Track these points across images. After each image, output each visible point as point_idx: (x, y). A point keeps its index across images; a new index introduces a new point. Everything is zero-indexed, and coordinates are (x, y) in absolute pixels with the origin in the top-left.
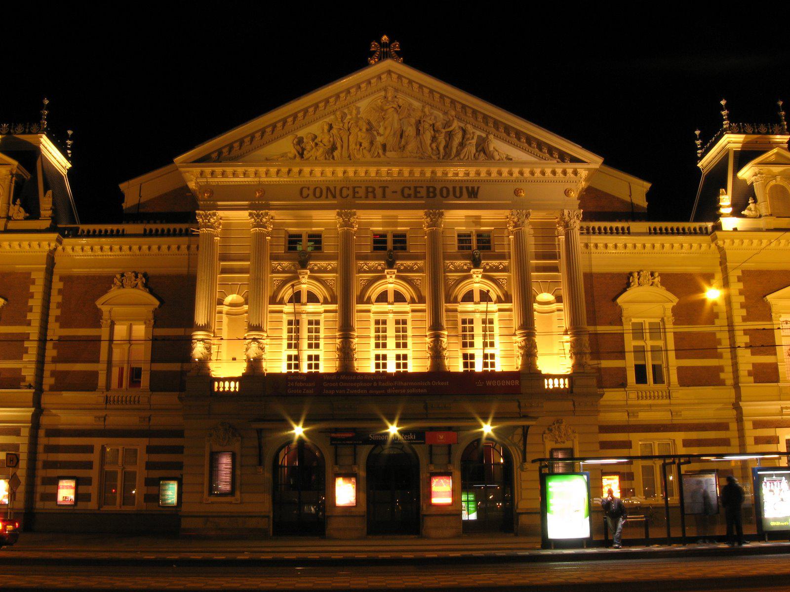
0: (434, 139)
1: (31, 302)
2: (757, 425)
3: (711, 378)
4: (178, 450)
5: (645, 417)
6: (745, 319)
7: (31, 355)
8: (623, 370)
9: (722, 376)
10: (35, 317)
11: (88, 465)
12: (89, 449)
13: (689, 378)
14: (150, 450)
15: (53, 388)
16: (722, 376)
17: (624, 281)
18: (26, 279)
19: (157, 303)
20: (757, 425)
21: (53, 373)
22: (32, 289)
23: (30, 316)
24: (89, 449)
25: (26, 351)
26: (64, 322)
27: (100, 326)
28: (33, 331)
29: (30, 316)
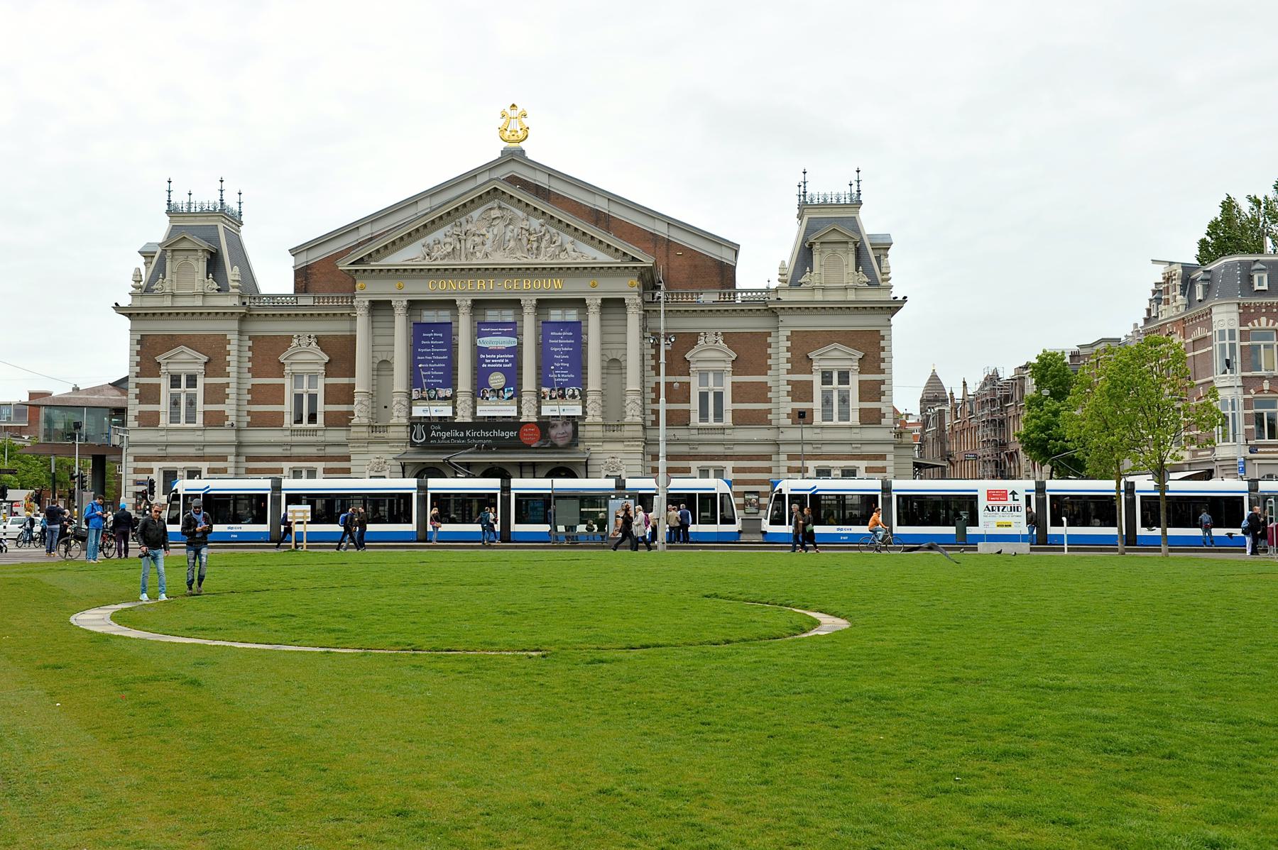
1: (228, 358)
2: (791, 457)
3: (760, 419)
6: (789, 372)
7: (231, 401)
9: (770, 417)
13: (742, 419)
15: (249, 424)
16: (770, 417)
20: (791, 457)
21: (249, 413)
22: (228, 348)
23: (228, 369)
26: (255, 373)
28: (232, 380)
29: (228, 369)
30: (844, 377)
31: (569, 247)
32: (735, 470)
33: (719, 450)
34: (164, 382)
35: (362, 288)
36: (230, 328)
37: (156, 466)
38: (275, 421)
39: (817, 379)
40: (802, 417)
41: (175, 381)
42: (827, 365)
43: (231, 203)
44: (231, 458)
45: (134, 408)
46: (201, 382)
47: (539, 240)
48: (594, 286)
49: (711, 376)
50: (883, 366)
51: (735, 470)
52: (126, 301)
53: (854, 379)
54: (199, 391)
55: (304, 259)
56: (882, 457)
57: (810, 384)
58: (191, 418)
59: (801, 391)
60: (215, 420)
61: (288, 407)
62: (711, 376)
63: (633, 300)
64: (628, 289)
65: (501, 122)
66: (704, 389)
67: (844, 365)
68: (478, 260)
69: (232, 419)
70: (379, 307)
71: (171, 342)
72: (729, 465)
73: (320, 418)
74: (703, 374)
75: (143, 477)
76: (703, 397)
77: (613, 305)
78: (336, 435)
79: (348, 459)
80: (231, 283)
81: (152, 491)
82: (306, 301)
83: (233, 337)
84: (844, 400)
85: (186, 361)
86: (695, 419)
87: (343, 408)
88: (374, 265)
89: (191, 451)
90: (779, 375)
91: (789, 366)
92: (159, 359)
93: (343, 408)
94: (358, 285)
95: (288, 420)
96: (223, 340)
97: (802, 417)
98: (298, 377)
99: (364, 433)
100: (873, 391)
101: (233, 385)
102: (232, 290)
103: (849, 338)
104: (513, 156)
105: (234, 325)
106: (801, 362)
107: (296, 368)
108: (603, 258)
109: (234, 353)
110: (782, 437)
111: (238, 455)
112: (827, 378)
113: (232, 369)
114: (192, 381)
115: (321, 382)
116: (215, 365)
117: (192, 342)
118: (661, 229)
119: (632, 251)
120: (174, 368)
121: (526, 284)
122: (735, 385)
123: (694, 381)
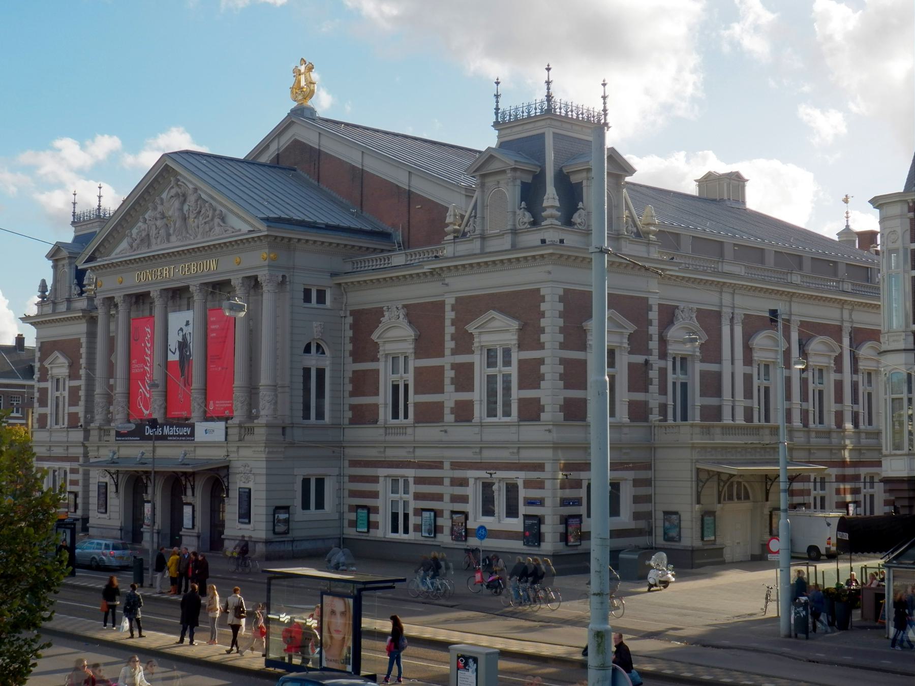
2: (455, 465)
5: (393, 454)
7: (82, 403)
18: (77, 343)
20: (455, 465)
25: (79, 398)
28: (81, 383)
31: (217, 220)
32: (419, 481)
33: (400, 454)
36: (79, 330)
39: (478, 360)
42: (488, 340)
50: (543, 338)
51: (419, 481)
52: (33, 311)
53: (515, 357)
54: (66, 394)
57: (471, 365)
65: (291, 81)
69: (82, 421)
72: (410, 473)
76: (395, 388)
83: (83, 340)
86: (385, 414)
97: (464, 412)
101: (83, 388)
104: (301, 114)
109: (84, 356)
110: (445, 437)
112: (491, 355)
113: (82, 372)
118: (400, 179)
122: (418, 371)
123: (383, 367)
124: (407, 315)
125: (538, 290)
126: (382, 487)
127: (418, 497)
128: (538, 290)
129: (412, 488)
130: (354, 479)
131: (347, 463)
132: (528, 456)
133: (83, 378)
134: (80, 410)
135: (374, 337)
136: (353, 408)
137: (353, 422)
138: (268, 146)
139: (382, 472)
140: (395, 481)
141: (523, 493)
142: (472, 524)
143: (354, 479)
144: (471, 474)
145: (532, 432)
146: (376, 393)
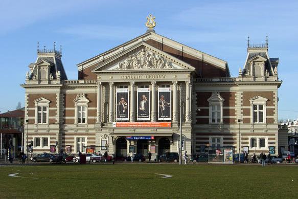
0: (153, 62)
1: (56, 101)
2: (242, 135)
4: (94, 138)
6: (242, 106)
8: (208, 119)
10: (58, 105)
11: (73, 142)
12: (73, 138)
14: (88, 138)
17: (209, 95)
18: (55, 95)
19: (88, 101)
20: (242, 135)
24: (73, 138)
27: (74, 107)
28: (58, 108)
30: (261, 107)
31: (166, 64)
34: (36, 109)
35: (100, 78)
37: (34, 137)
38: (72, 122)
40: (246, 121)
41: (39, 109)
43: (58, 50)
44: (58, 134)
45: (27, 117)
46: (48, 109)
47: (157, 62)
48: (176, 77)
49: (216, 107)
51: (224, 139)
54: (47, 112)
55: (80, 68)
56: (274, 135)
58: (44, 121)
59: (246, 112)
60: (52, 122)
61: (75, 118)
62: (216, 107)
63: (188, 81)
64: (186, 78)
66: (214, 111)
67: (261, 103)
68: (136, 69)
69: (58, 121)
70: (105, 84)
71: (38, 96)
72: (222, 137)
73: (86, 121)
74: (213, 106)
75: (29, 140)
77: (181, 84)
78: (91, 126)
79: (94, 135)
80: (57, 76)
81: (32, 145)
82: (82, 82)
83: (58, 94)
84: (261, 114)
85: (44, 102)
87: (93, 118)
88: (103, 71)
89: (45, 132)
90: (238, 107)
91: (242, 103)
92: (35, 102)
93: (93, 118)
94: (98, 77)
95: (76, 122)
96: (55, 95)
98: (79, 108)
99: (99, 126)
100: (270, 112)
102: (58, 79)
103: (263, 94)
105: (58, 90)
106: (246, 102)
107: (79, 104)
108: (179, 68)
111: (60, 133)
114: (45, 109)
115: (86, 109)
116: (52, 103)
117: (46, 96)
119: (188, 66)
120: (39, 104)
121: (152, 76)
123: (210, 109)
124: (221, 95)
125: (273, 92)
126: (210, 141)
127: (224, 143)
128: (273, 92)
129: (222, 141)
130: (197, 139)
131: (195, 134)
132: (269, 132)
133: (58, 107)
134: (57, 118)
135: (208, 100)
136: (197, 119)
137: (197, 123)
138: (138, 40)
139: (210, 137)
140: (214, 140)
141: (267, 141)
142: (250, 149)
143: (197, 139)
144: (250, 137)
145: (270, 126)
146: (208, 115)
